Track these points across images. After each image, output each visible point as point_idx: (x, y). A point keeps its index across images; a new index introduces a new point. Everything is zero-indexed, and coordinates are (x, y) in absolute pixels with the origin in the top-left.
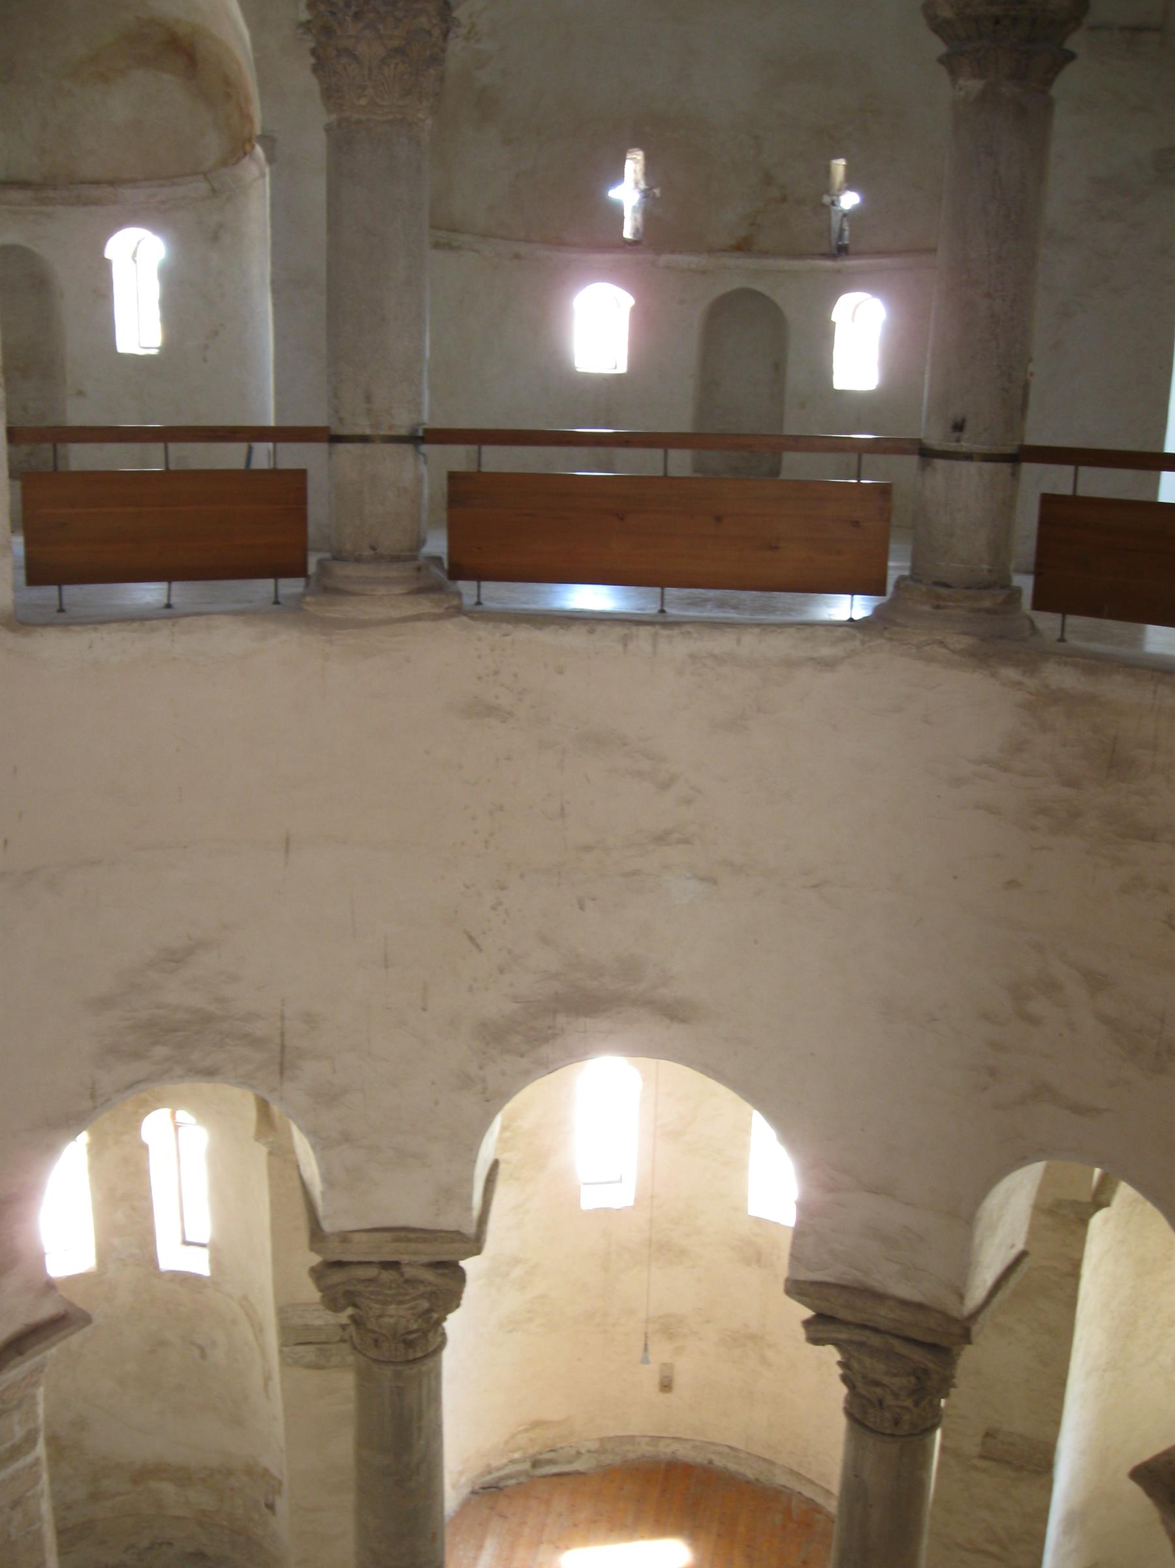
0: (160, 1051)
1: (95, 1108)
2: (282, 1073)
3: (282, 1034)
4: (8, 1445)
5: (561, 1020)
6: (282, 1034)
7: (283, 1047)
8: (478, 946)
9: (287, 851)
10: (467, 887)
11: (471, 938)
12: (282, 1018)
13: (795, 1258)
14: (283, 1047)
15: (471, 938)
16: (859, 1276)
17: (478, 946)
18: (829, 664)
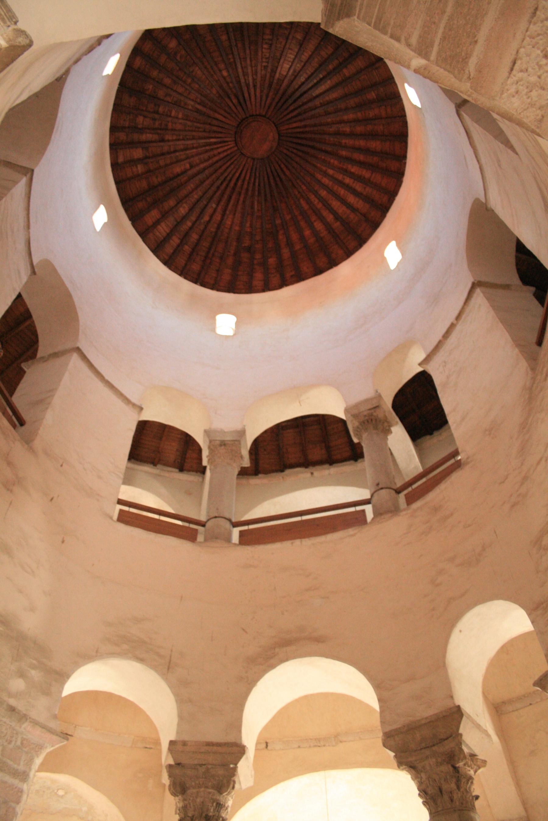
0: (125, 646)
1: (96, 656)
2: (168, 669)
3: (171, 657)
4: (16, 766)
5: (277, 650)
6: (171, 657)
7: (170, 661)
8: (246, 632)
9: (181, 599)
10: (243, 614)
11: (244, 630)
12: (172, 651)
13: (383, 722)
14: (170, 661)
15: (244, 630)
16: (411, 719)
17: (246, 632)
18: (352, 535)
